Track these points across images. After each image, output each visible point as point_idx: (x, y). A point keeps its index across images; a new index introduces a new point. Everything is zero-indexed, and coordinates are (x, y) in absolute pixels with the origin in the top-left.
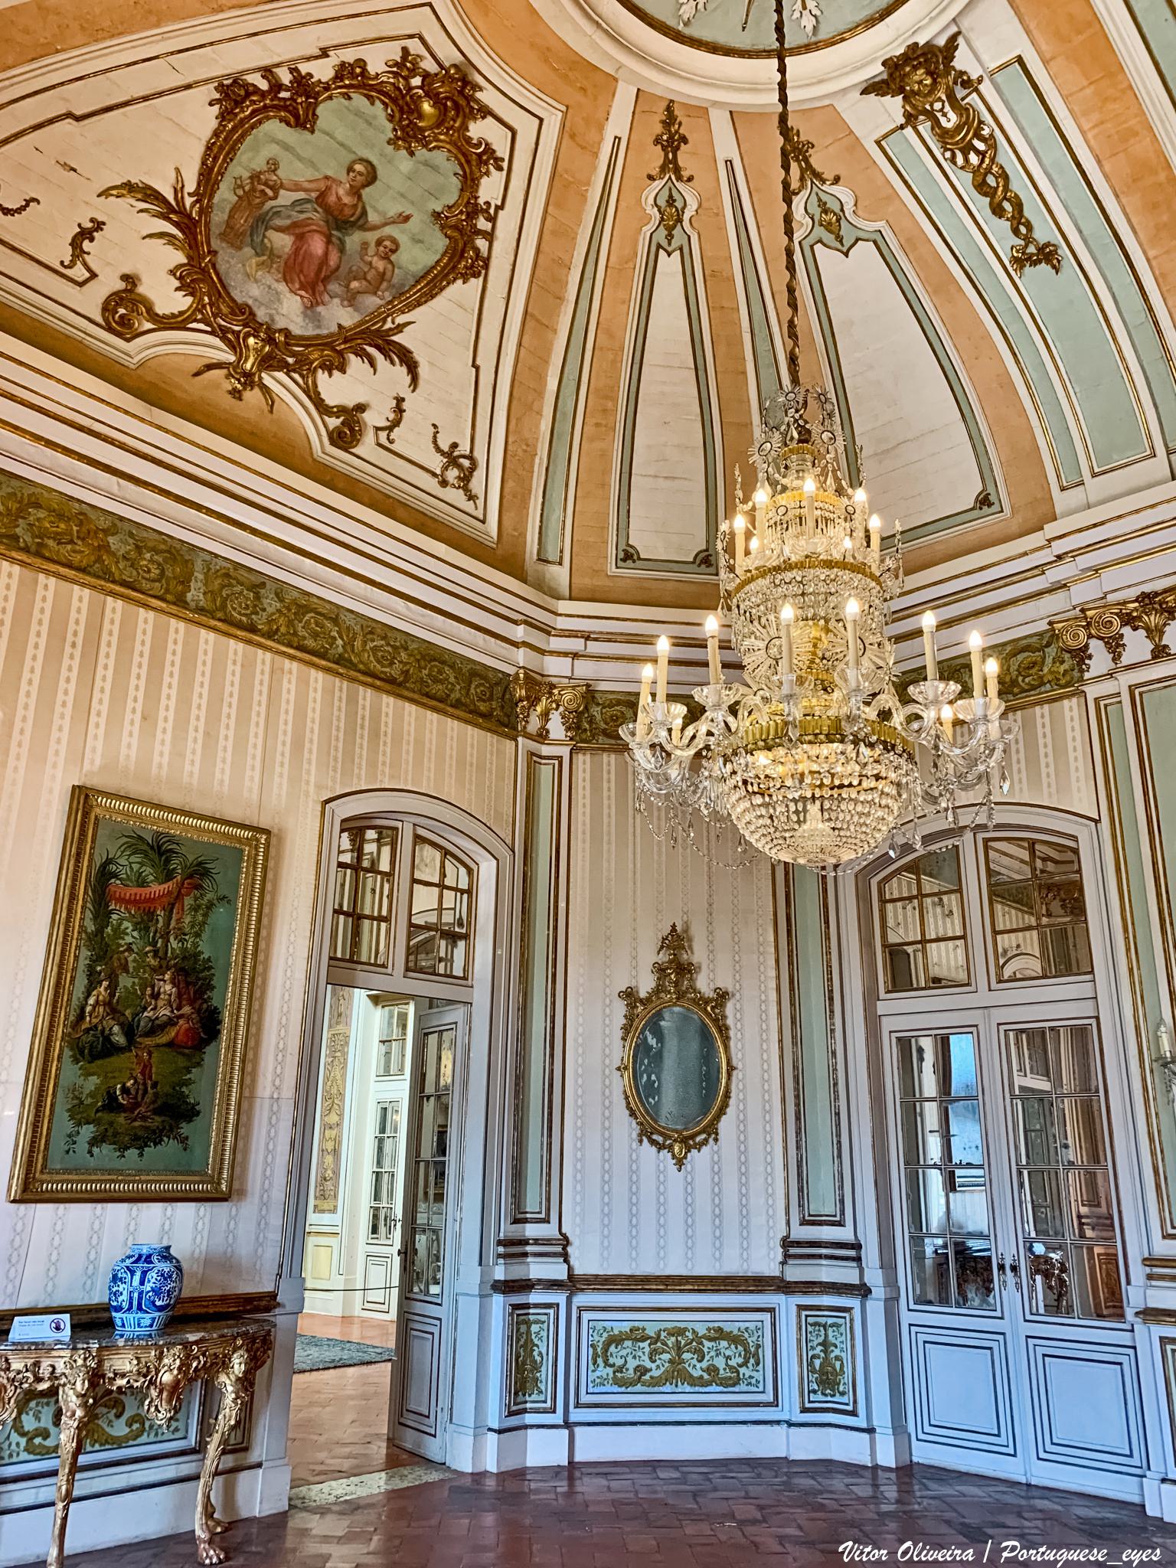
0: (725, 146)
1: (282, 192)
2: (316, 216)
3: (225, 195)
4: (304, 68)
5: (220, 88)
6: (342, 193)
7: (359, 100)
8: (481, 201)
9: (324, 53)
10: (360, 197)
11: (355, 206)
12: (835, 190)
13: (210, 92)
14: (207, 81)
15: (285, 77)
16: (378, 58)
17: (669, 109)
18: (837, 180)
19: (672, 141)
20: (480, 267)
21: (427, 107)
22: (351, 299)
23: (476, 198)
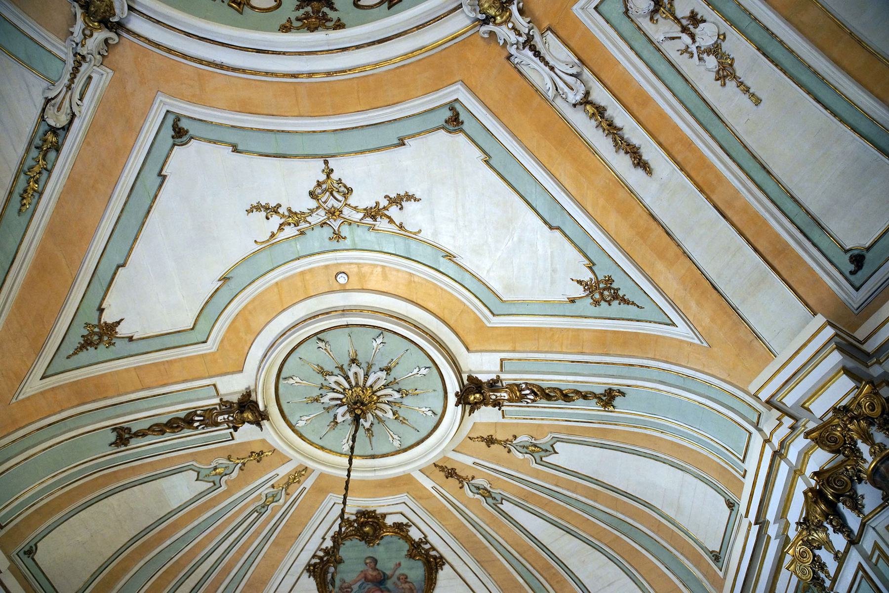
0: (468, 460)
1: (353, 587)
2: (370, 586)
4: (324, 547)
5: (308, 571)
8: (417, 540)
9: (324, 539)
10: (377, 570)
11: (379, 573)
12: (518, 440)
13: (306, 575)
14: (302, 572)
15: (321, 554)
17: (435, 465)
18: (515, 437)
19: (451, 473)
23: (414, 541)
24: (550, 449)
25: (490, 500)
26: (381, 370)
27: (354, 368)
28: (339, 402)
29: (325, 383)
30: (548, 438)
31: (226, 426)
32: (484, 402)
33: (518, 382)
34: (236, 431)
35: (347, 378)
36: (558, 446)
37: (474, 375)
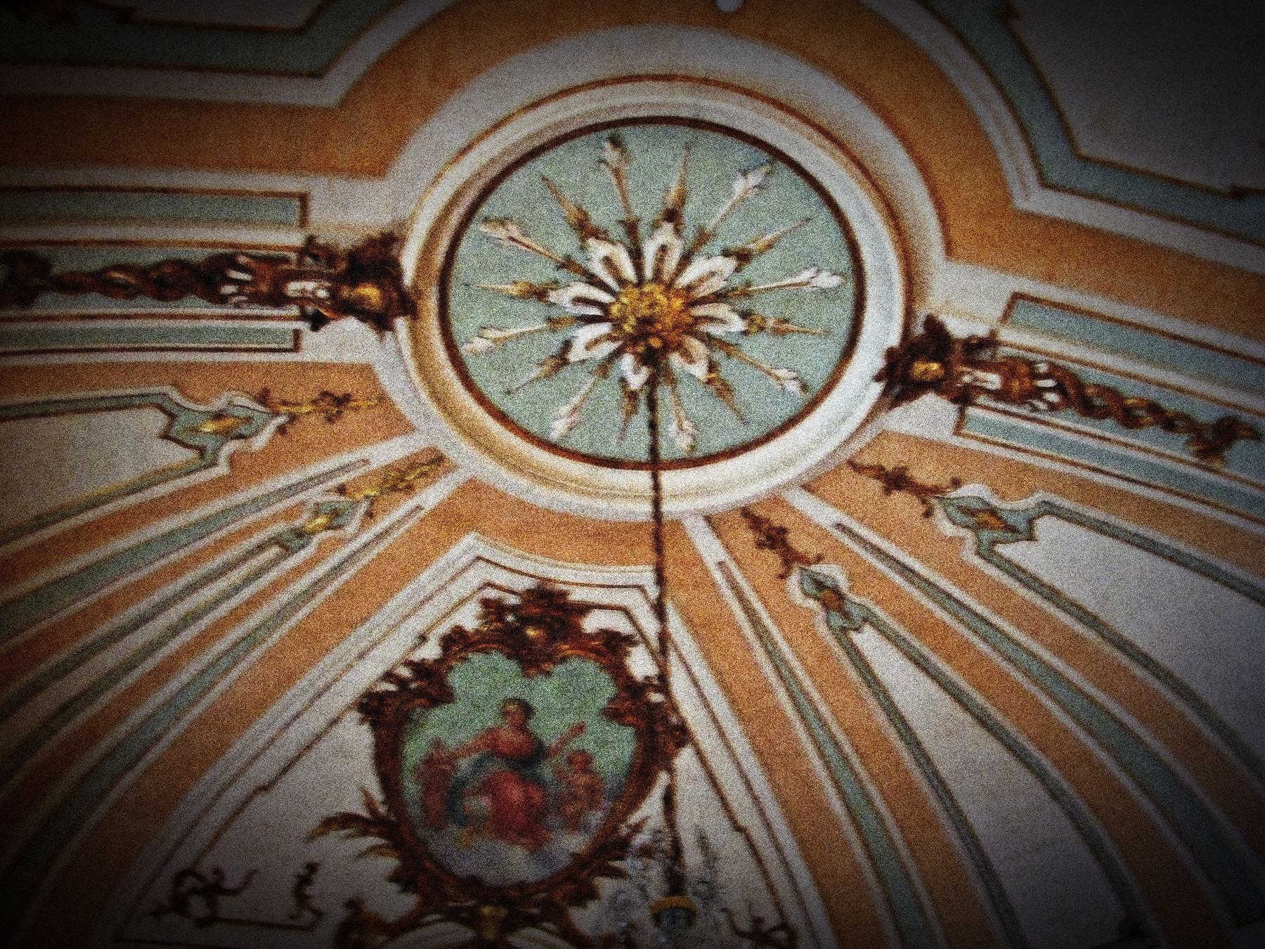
3: (411, 788)
4: (418, 656)
6: (508, 735)
7: (476, 658)
9: (423, 638)
15: (405, 672)
16: (469, 619)
20: (682, 735)
21: (531, 633)
22: (575, 824)
24: (1022, 526)
25: (837, 621)
26: (726, 253)
27: (665, 235)
28: (595, 311)
29: (578, 257)
30: (1028, 503)
31: (295, 311)
32: (936, 386)
33: (1031, 356)
34: (315, 328)
35: (636, 256)
36: (1045, 526)
37: (942, 317)
